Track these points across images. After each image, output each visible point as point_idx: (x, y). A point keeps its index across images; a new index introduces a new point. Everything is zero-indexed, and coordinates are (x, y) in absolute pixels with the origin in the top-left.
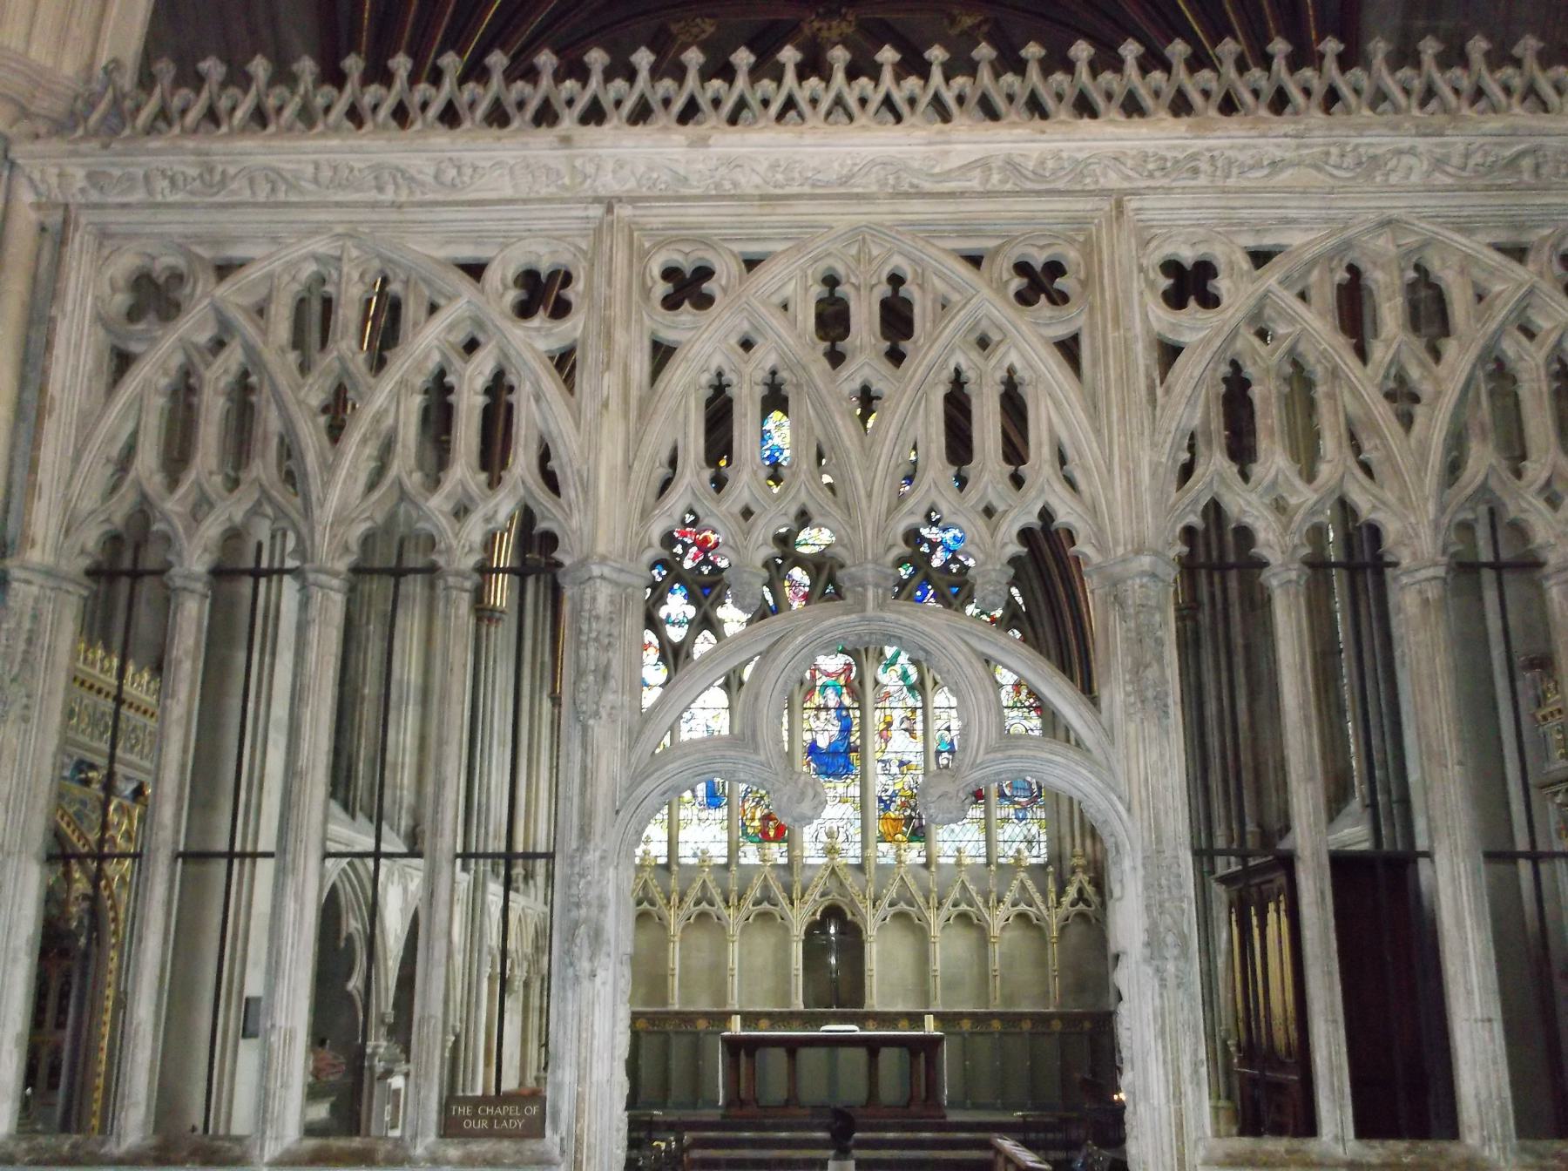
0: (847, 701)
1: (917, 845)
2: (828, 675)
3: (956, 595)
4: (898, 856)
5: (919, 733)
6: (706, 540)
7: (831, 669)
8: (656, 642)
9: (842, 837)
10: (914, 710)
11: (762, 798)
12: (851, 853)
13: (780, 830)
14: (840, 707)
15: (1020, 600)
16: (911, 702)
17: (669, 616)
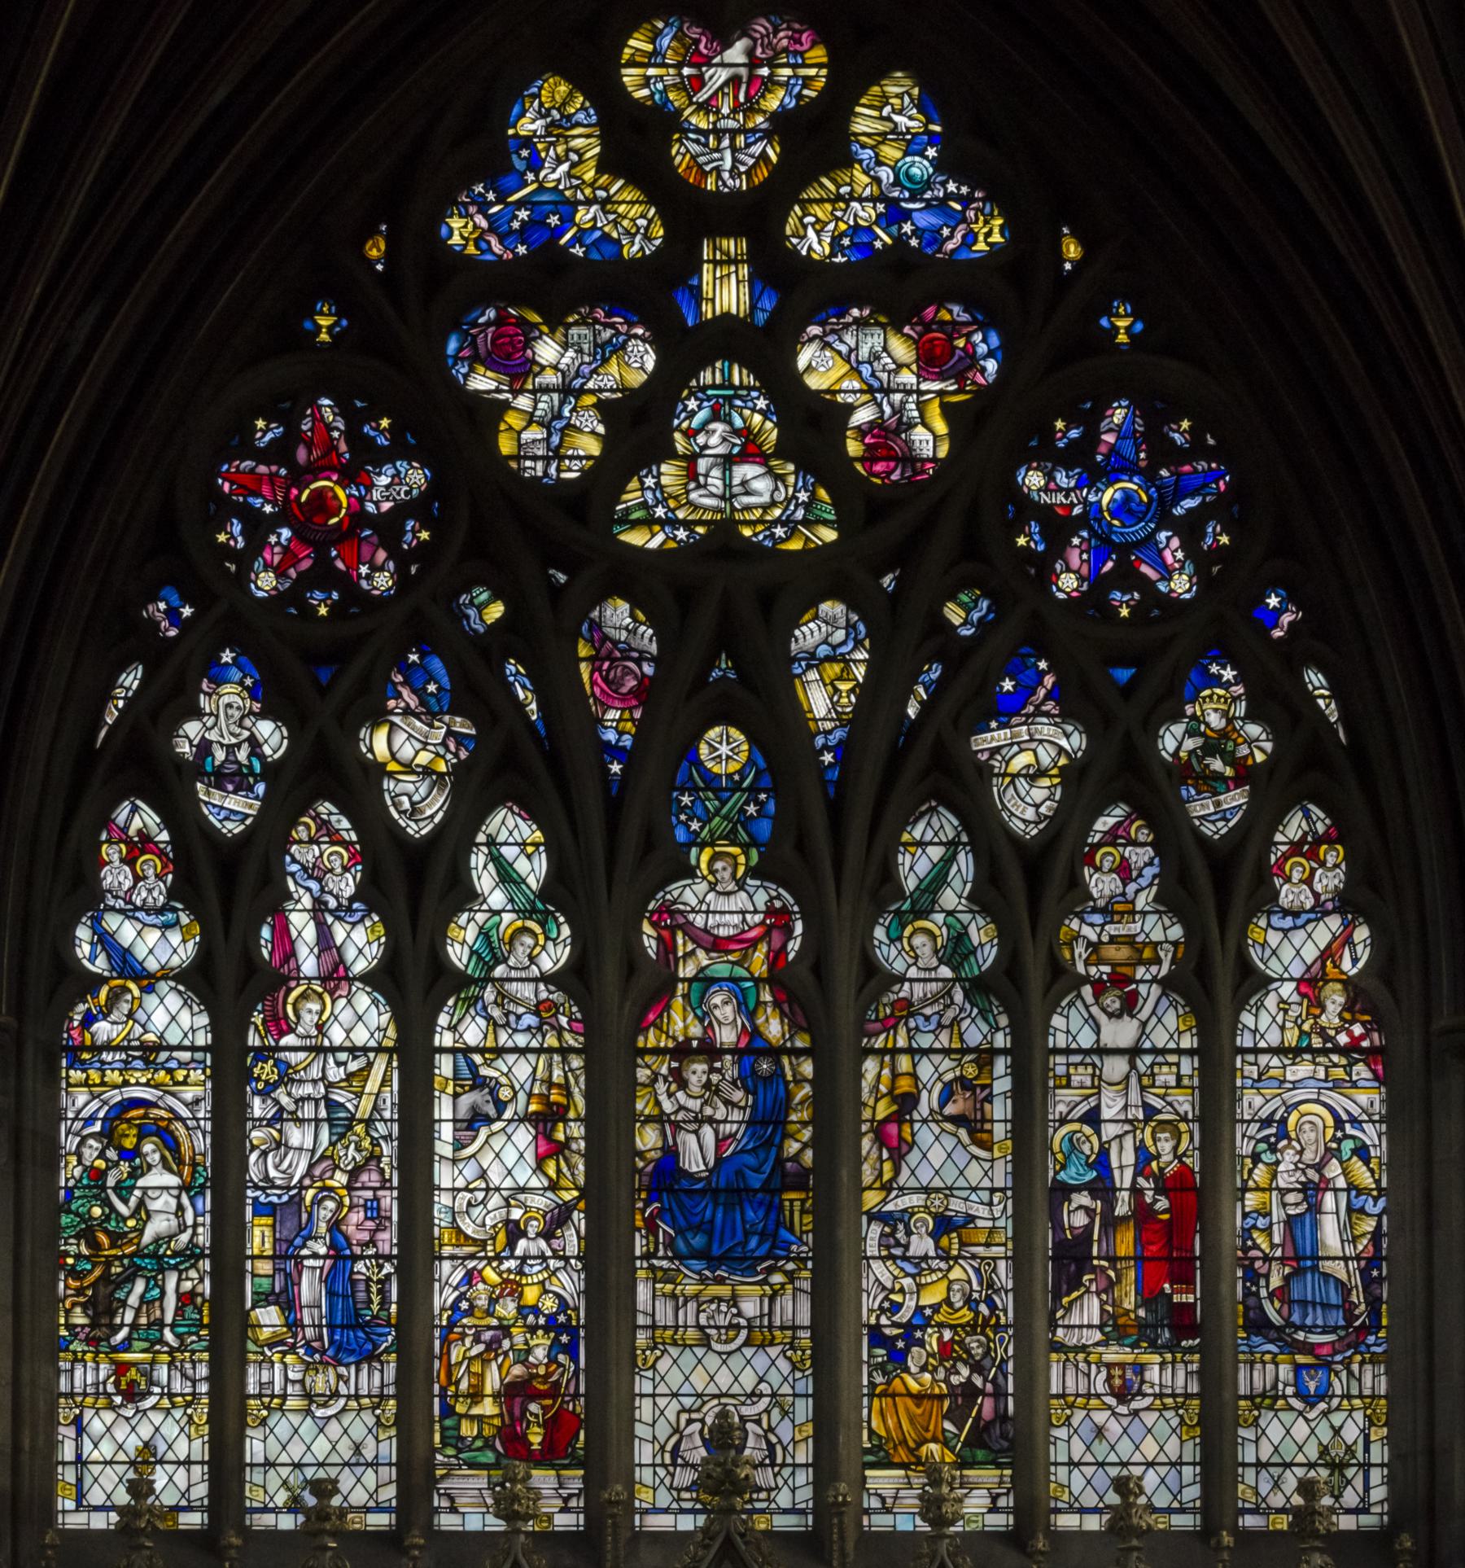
0: (774, 1028)
1: (987, 1475)
2: (717, 945)
3: (1128, 691)
4: (933, 1508)
5: (999, 1131)
6: (323, 503)
7: (726, 926)
9: (753, 1449)
10: (985, 1056)
11: (505, 1330)
12: (784, 1499)
13: (557, 1427)
14: (753, 1047)
15: (1332, 713)
16: (974, 1035)
17: (205, 748)
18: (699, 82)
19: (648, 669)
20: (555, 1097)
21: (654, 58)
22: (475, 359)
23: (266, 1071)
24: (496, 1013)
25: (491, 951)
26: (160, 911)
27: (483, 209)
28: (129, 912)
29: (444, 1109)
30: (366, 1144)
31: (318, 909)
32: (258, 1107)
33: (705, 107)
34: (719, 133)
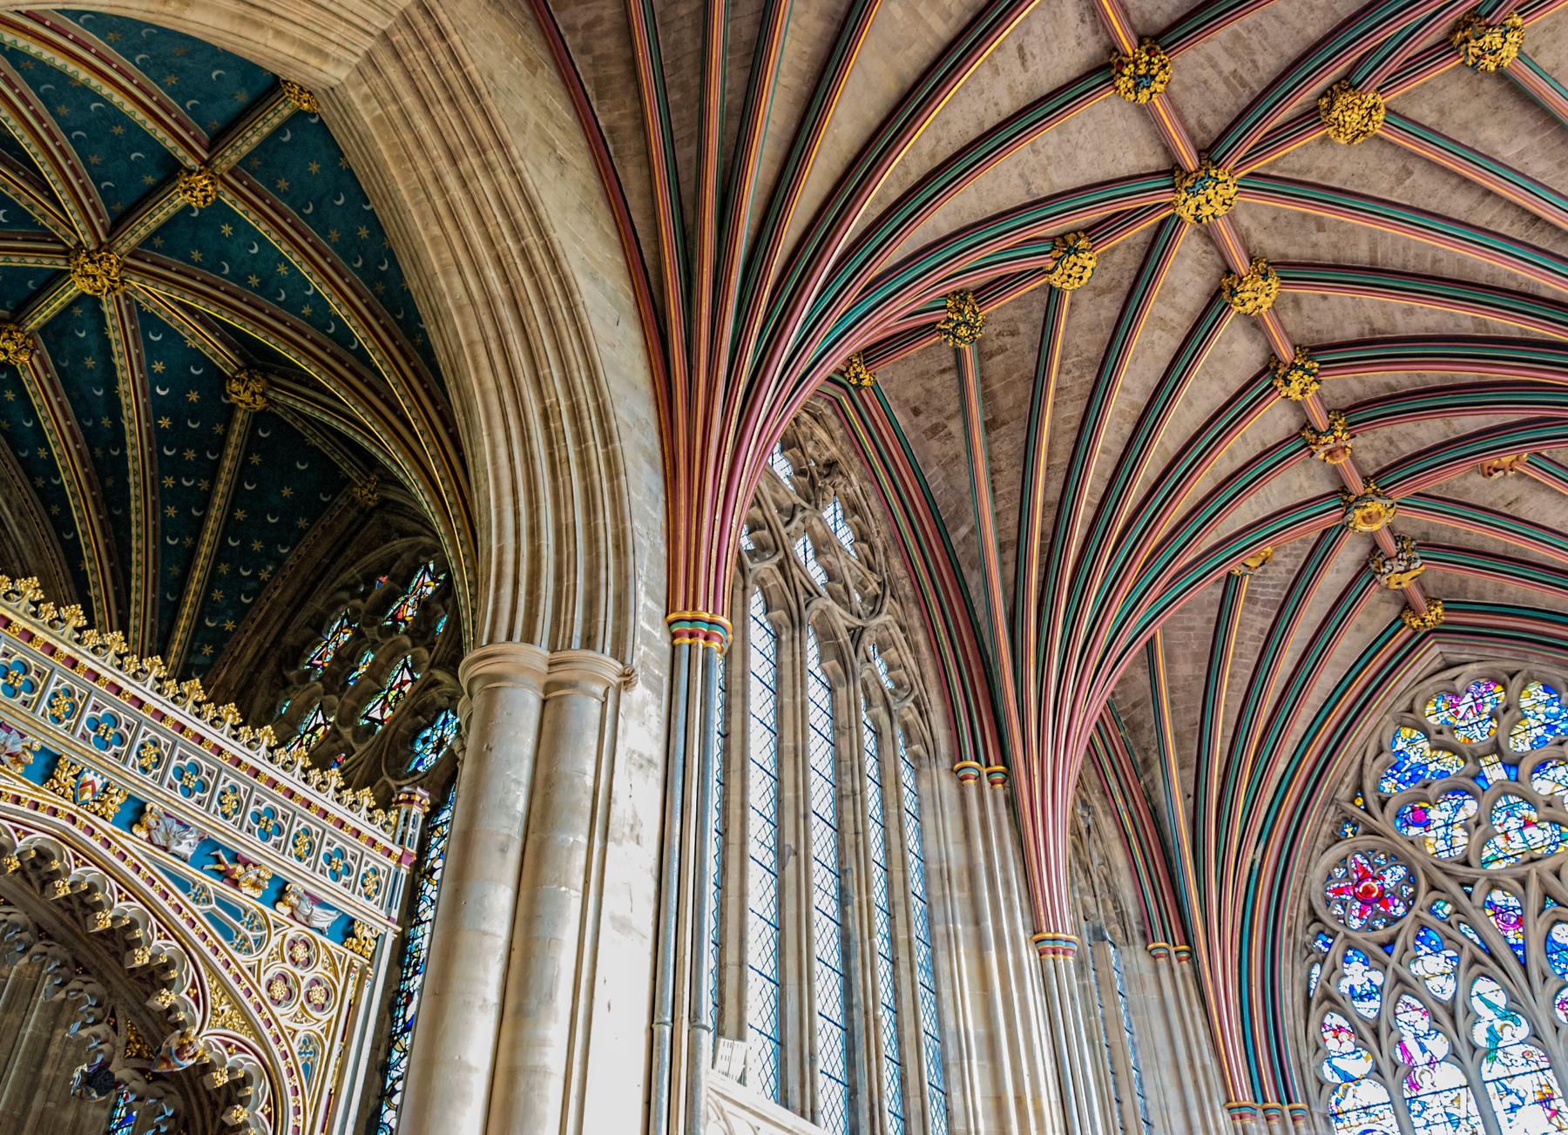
6: (1368, 890)
8: (1345, 1024)
17: (1352, 988)
18: (1457, 713)
19: (1519, 912)
20: (1545, 1090)
21: (1438, 710)
22: (1408, 825)
23: (1416, 1107)
24: (1504, 1060)
25: (1494, 1036)
26: (1353, 1053)
27: (1393, 776)
28: (1342, 1056)
29: (1496, 1103)
30: (1469, 1128)
31: (1416, 1036)
32: (1419, 1122)
33: (1463, 719)
34: (1471, 725)
